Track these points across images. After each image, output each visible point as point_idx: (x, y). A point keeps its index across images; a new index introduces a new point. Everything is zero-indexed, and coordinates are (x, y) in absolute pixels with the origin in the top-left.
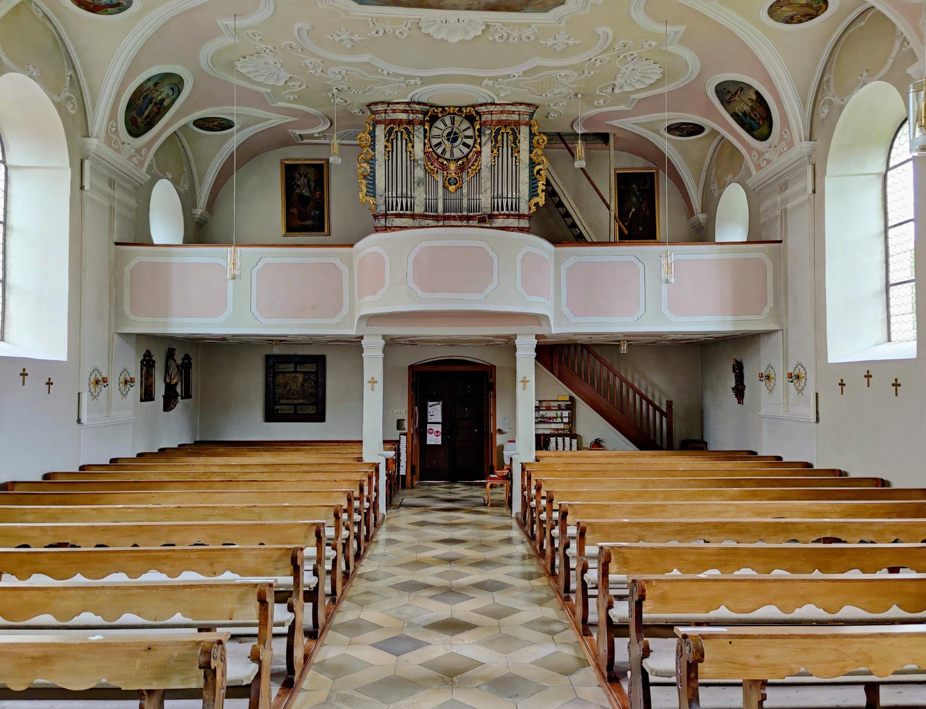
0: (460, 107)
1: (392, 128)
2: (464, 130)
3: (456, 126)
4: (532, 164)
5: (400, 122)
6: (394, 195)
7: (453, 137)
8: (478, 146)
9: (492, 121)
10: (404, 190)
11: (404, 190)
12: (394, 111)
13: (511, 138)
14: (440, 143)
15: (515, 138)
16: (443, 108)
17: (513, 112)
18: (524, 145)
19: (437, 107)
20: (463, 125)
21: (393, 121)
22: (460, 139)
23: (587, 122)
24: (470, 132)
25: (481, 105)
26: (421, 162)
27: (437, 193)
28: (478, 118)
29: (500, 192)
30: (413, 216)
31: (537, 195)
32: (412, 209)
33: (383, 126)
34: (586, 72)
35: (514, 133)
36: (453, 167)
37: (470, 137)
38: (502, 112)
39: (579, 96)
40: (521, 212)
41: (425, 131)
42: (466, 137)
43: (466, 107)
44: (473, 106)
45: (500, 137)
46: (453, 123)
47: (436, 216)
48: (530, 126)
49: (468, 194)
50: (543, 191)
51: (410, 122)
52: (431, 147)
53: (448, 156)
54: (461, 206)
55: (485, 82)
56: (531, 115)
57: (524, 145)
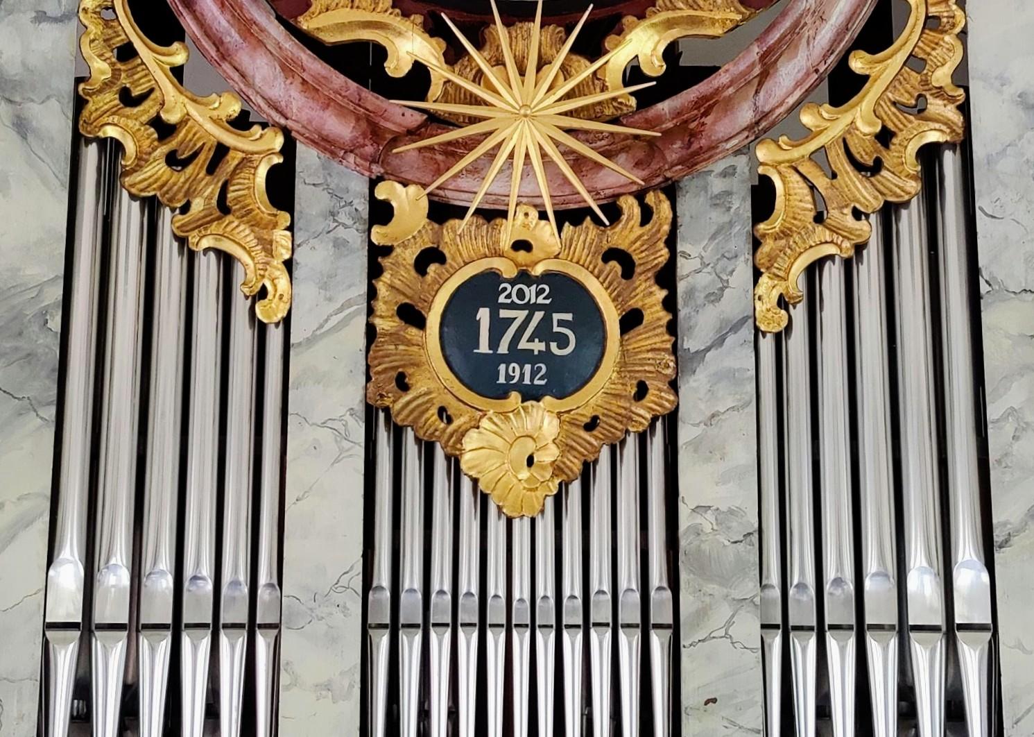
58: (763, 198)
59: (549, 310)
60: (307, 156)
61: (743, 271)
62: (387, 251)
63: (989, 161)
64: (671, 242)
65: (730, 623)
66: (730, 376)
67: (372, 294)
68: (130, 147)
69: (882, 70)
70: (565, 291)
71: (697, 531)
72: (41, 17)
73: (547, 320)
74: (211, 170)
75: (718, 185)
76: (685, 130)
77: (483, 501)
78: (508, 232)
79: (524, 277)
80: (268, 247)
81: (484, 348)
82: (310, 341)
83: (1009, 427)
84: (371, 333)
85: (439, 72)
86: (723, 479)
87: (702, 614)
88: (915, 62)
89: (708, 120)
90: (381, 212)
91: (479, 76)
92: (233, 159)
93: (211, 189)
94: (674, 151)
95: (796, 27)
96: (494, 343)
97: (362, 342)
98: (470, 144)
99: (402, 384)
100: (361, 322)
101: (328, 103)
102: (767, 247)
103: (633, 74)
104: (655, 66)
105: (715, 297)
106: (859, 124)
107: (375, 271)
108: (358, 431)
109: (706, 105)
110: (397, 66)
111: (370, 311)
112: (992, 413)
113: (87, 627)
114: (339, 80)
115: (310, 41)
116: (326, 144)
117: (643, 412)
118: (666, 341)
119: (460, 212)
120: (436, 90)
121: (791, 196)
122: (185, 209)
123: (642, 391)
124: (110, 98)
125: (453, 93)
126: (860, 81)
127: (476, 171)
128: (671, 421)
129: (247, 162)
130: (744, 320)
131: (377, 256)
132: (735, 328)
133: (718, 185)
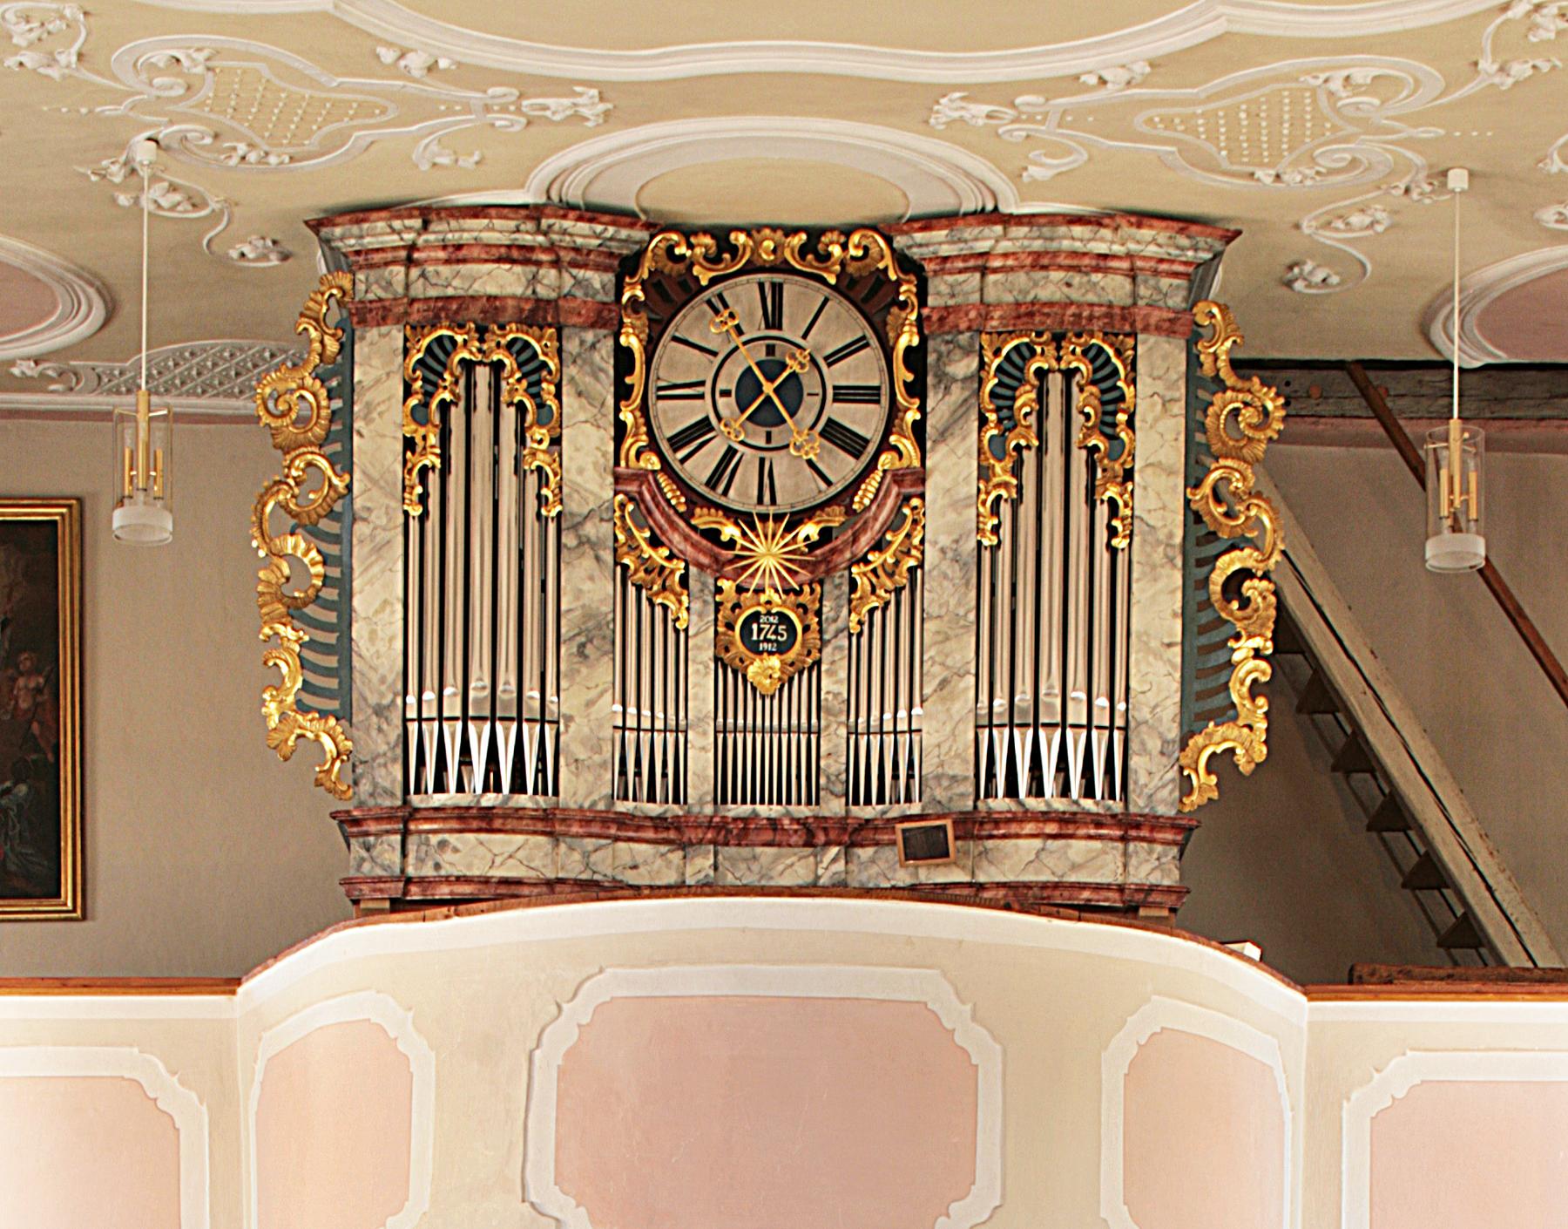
0: (815, 233)
1: (445, 346)
4: (1201, 540)
5: (487, 315)
6: (453, 708)
7: (769, 395)
8: (908, 446)
9: (986, 309)
10: (507, 678)
11: (507, 678)
12: (456, 254)
14: (704, 426)
15: (1112, 401)
16: (721, 235)
18: (1157, 439)
19: (688, 233)
20: (822, 325)
21: (449, 309)
23: (1503, 310)
24: (863, 369)
25: (928, 222)
27: (682, 698)
28: (907, 291)
29: (1024, 697)
30: (549, 823)
31: (1227, 713)
32: (548, 784)
34: (1487, 65)
35: (1104, 376)
36: (768, 554)
37: (868, 395)
38: (1040, 262)
39: (1458, 180)
40: (1138, 804)
41: (623, 359)
42: (844, 394)
43: (847, 232)
44: (885, 228)
45: (1025, 399)
47: (677, 824)
48: (1193, 338)
49: (850, 705)
50: (1255, 690)
51: (539, 313)
53: (742, 493)
54: (813, 769)
55: (947, 109)
56: (1198, 278)
57: (1157, 439)
60: (693, 570)
61: (845, 611)
68: (632, 567)
70: (783, 618)
72: (602, 520)
74: (660, 574)
76: (825, 559)
77: (754, 689)
78: (763, 598)
80: (680, 602)
81: (755, 637)
84: (716, 632)
85: (740, 542)
86: (836, 682)
87: (828, 727)
88: (908, 536)
90: (719, 590)
91: (752, 542)
93: (660, 582)
94: (823, 568)
95: (865, 522)
99: (727, 650)
103: (807, 538)
104: (815, 537)
105: (835, 620)
107: (717, 611)
108: (712, 666)
109: (833, 551)
110: (725, 538)
113: (624, 728)
114: (704, 542)
115: (694, 528)
116: (700, 566)
119: (747, 590)
124: (625, 549)
125: (744, 548)
127: (753, 576)
129: (672, 572)
131: (718, 606)
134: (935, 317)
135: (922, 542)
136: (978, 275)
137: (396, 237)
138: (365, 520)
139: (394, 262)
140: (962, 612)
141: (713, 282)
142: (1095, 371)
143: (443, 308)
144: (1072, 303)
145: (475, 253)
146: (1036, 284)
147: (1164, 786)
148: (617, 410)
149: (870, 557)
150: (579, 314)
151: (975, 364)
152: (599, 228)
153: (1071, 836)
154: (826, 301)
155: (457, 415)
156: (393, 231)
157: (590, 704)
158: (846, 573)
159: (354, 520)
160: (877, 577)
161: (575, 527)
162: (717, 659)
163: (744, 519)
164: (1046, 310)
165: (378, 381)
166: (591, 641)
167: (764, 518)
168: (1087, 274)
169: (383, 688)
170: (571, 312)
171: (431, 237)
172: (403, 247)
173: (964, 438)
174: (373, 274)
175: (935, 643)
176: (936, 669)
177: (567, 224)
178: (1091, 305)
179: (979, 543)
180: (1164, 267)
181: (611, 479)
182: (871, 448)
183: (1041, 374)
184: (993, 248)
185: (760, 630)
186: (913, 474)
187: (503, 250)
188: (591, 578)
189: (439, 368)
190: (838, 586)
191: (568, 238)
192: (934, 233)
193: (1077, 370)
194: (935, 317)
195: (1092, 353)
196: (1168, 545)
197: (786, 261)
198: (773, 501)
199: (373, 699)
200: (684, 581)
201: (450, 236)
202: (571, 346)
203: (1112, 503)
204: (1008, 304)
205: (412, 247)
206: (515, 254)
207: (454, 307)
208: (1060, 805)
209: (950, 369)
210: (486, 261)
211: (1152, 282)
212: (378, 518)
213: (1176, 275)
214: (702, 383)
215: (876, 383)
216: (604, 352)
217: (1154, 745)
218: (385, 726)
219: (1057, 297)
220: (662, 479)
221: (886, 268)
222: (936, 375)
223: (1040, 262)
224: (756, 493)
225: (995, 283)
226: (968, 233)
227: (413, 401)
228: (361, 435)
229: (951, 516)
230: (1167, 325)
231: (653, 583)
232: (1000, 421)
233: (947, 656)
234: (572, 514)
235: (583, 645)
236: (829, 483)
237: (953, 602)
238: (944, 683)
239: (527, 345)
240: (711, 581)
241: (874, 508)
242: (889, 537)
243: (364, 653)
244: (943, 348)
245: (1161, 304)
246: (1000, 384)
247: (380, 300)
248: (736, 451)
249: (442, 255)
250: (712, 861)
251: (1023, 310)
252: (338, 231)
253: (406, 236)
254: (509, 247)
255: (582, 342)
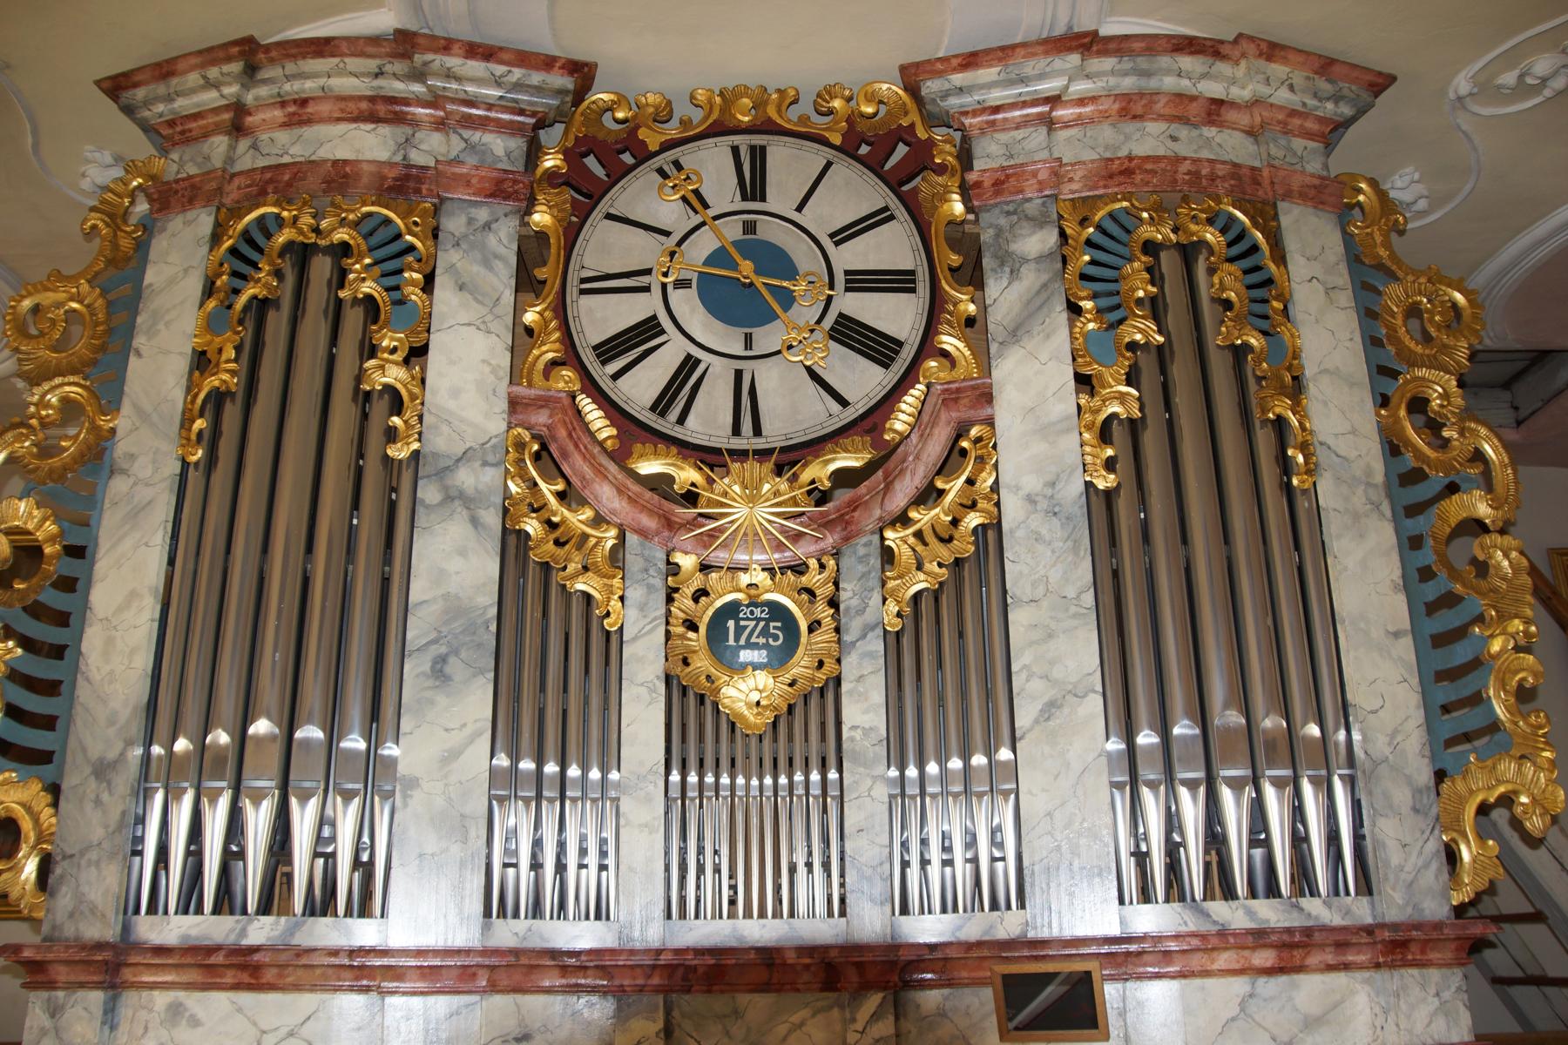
2: (842, 236)
3: (772, 204)
9: (1058, 173)
12: (299, 112)
13: (1230, 283)
14: (648, 330)
17: (1215, 110)
21: (280, 182)
22: (806, 311)
24: (892, 247)
26: (476, 479)
28: (945, 155)
33: (205, 221)
35: (1241, 250)
37: (898, 281)
38: (1131, 108)
42: (860, 281)
46: (754, 186)
52: (570, 356)
53: (709, 419)
58: (888, 556)
59: (768, 621)
60: (632, 539)
61: (876, 598)
62: (676, 590)
63: (1011, 531)
64: (836, 584)
65: (870, 790)
66: (871, 655)
67: (668, 613)
69: (954, 487)
70: (777, 611)
71: (852, 739)
72: (485, 464)
73: (767, 626)
75: (862, 551)
79: (753, 604)
80: (610, 590)
81: (731, 642)
82: (635, 639)
83: (1024, 675)
84: (668, 635)
86: (866, 711)
88: (970, 482)
89: (856, 514)
90: (673, 569)
92: (593, 541)
96: (737, 639)
97: (663, 639)
98: (721, 530)
99: (686, 662)
100: (662, 629)
101: (643, 509)
102: (891, 584)
106: (942, 516)
107: (670, 600)
111: (668, 623)
112: (1014, 668)
116: (643, 533)
117: (821, 676)
118: (832, 636)
120: (702, 501)
121: (904, 553)
122: (565, 568)
123: (821, 664)
124: (525, 509)
126: (941, 493)
128: (838, 681)
130: (877, 625)
132: (873, 628)
133: (862, 551)
134: (987, 184)
135: (995, 488)
136: (1043, 130)
137: (214, 94)
138: (124, 472)
139: (217, 129)
140: (1071, 592)
141: (667, 146)
142: (1230, 245)
143: (271, 181)
144: (1185, 159)
145: (325, 108)
146: (1127, 138)
147: (1426, 866)
148: (518, 311)
149: (913, 514)
150: (468, 184)
151: (1052, 238)
152: (500, 69)
153: (1300, 969)
154: (829, 165)
155: (277, 323)
156: (210, 84)
157: (452, 755)
158: (876, 538)
159: (112, 472)
160: (925, 544)
161: (442, 473)
162: (668, 679)
163: (710, 458)
164: (1149, 166)
165: (172, 281)
166: (456, 652)
167: (741, 455)
168: (1195, 126)
169: (111, 731)
170: (457, 178)
171: (263, 91)
172: (227, 108)
173: (1048, 336)
174: (189, 151)
175: (1032, 644)
176: (1036, 685)
177: (454, 62)
178: (1209, 161)
179: (1089, 485)
180: (1296, 122)
181: (505, 405)
182: (907, 354)
183: (1150, 247)
184: (1067, 87)
185: (739, 630)
186: (973, 388)
187: (364, 105)
188: (463, 552)
189: (254, 255)
190: (861, 560)
191: (454, 86)
192: (981, 72)
193: (1203, 243)
194: (987, 184)
195: (1221, 222)
196: (1368, 484)
197: (770, 120)
198: (757, 431)
199: (96, 750)
200: (616, 557)
201: (287, 87)
202: (453, 224)
203: (1280, 423)
204: (1092, 161)
205: (239, 109)
206: (382, 109)
207: (287, 177)
208: (1269, 913)
209: (1014, 247)
210: (339, 120)
211: (1283, 142)
212: (143, 468)
213: (1309, 135)
214: (648, 272)
215: (908, 266)
216: (503, 234)
217: (1402, 796)
218: (105, 797)
219: (1161, 152)
220: (586, 404)
221: (912, 125)
222: (995, 256)
223: (1131, 108)
224: (729, 419)
225: (1068, 140)
226: (1031, 67)
227: (212, 304)
228: (139, 354)
229: (1039, 448)
230: (1313, 192)
231: (568, 559)
232: (1099, 311)
233: (1052, 663)
234: (436, 455)
235: (443, 659)
236: (844, 403)
237: (1055, 575)
238: (1050, 709)
239: (387, 221)
240: (661, 555)
241: (914, 438)
242: (940, 484)
243: (96, 676)
244: (1003, 221)
245: (1298, 167)
246: (1093, 262)
247: (190, 177)
248: (698, 361)
249: (278, 114)
250: (660, 1024)
251: (1115, 166)
252: (140, 93)
253: (227, 90)
254: (372, 99)
255: (470, 221)
